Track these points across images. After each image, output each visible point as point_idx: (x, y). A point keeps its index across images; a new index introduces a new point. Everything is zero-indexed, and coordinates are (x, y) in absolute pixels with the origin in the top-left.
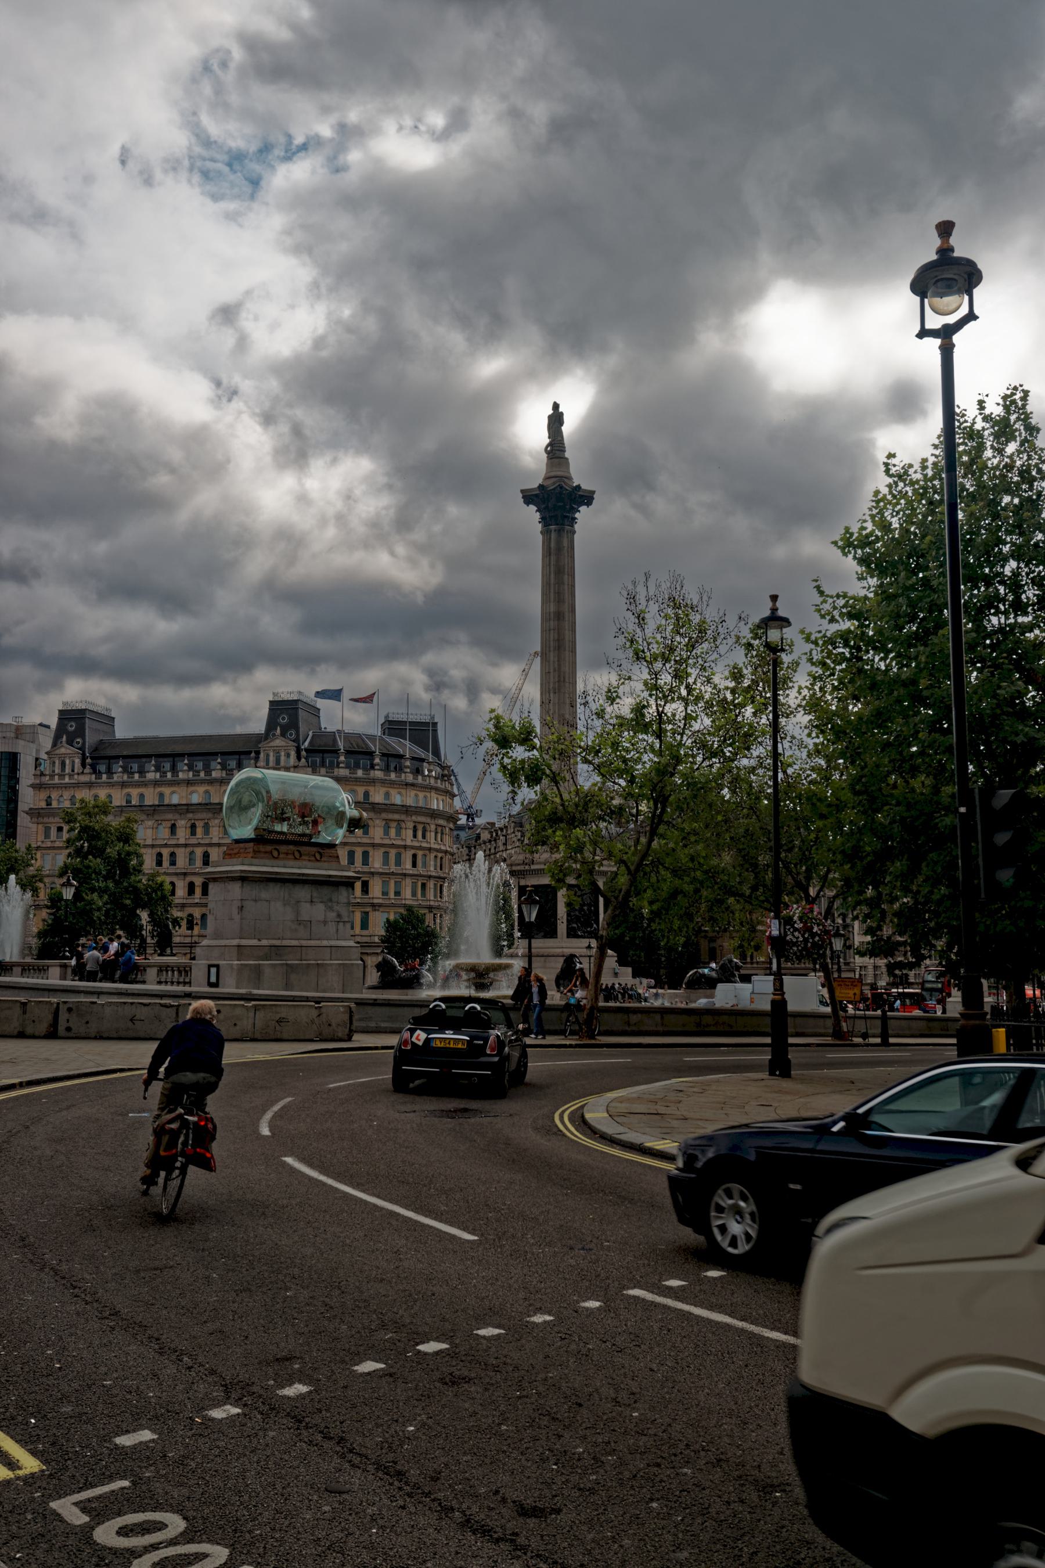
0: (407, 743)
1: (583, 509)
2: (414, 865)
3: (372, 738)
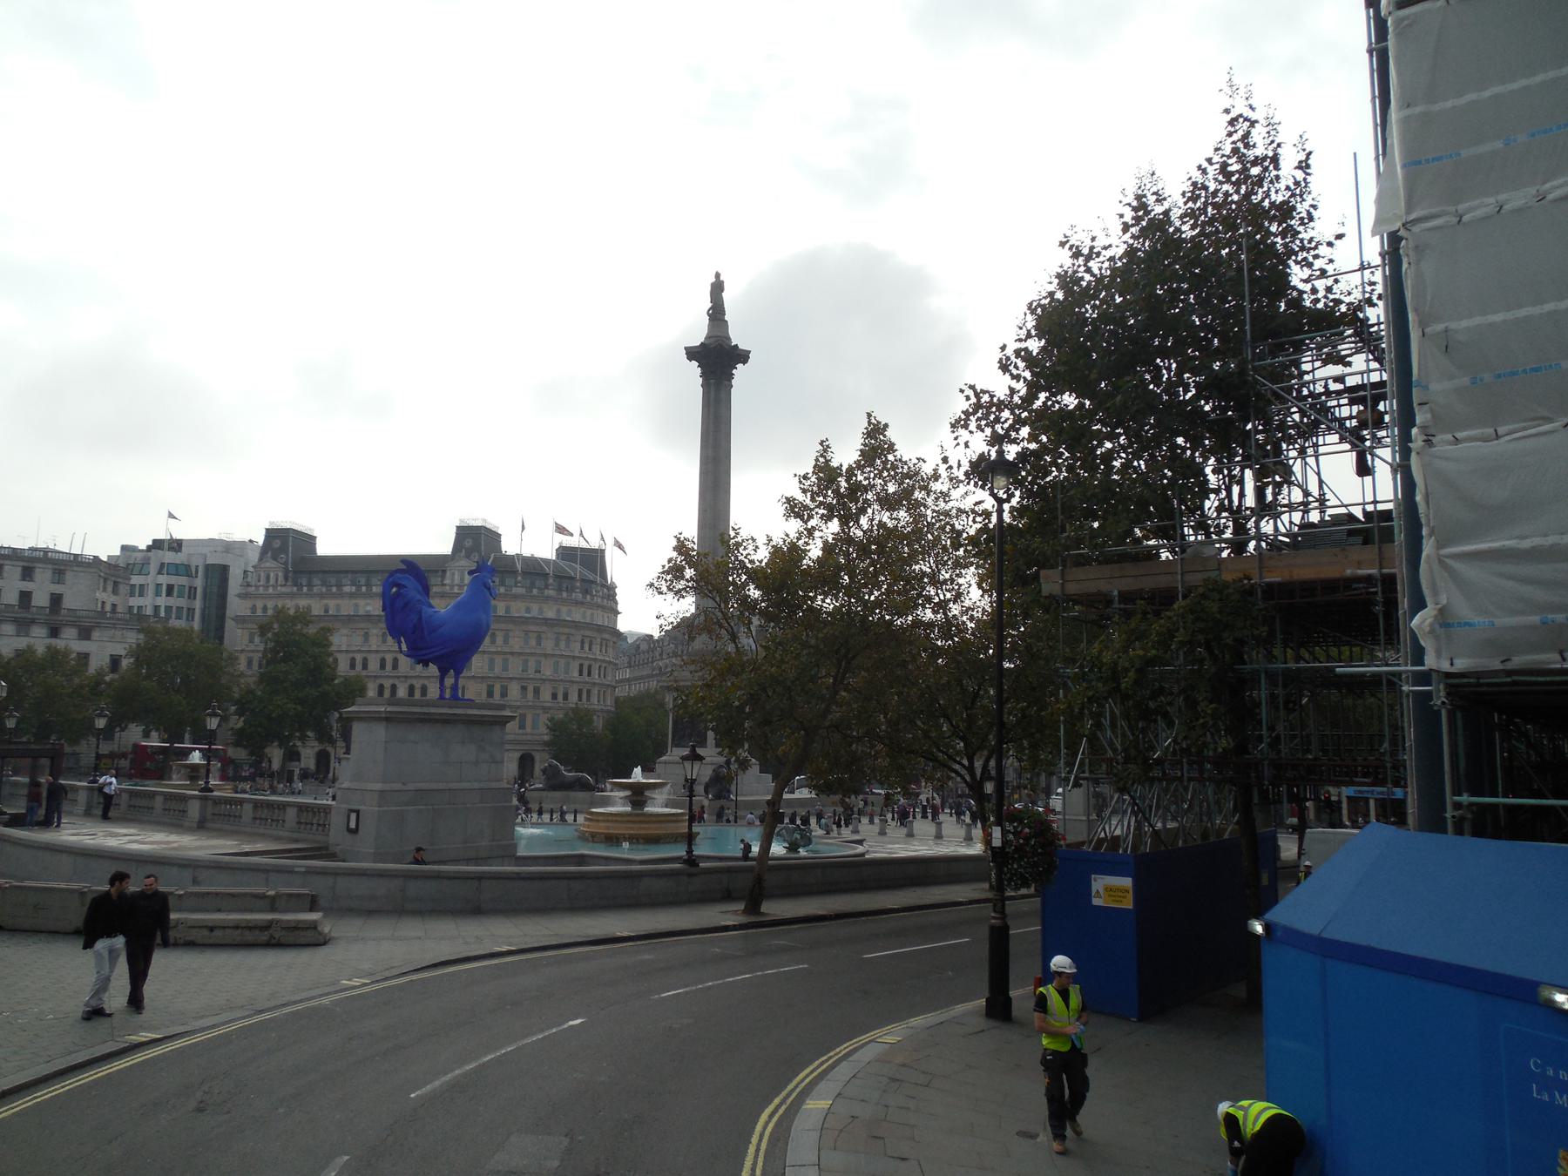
0: (578, 566)
1: (739, 366)
2: (581, 674)
3: (546, 561)
